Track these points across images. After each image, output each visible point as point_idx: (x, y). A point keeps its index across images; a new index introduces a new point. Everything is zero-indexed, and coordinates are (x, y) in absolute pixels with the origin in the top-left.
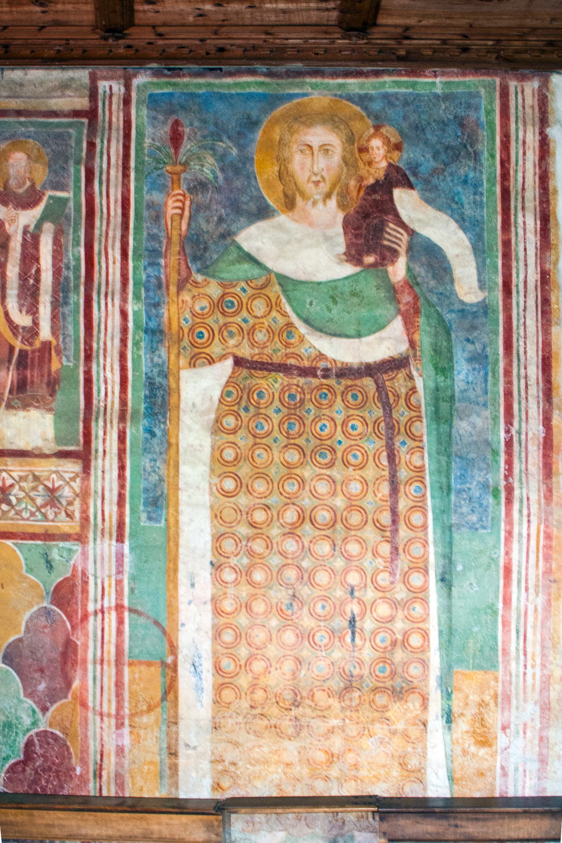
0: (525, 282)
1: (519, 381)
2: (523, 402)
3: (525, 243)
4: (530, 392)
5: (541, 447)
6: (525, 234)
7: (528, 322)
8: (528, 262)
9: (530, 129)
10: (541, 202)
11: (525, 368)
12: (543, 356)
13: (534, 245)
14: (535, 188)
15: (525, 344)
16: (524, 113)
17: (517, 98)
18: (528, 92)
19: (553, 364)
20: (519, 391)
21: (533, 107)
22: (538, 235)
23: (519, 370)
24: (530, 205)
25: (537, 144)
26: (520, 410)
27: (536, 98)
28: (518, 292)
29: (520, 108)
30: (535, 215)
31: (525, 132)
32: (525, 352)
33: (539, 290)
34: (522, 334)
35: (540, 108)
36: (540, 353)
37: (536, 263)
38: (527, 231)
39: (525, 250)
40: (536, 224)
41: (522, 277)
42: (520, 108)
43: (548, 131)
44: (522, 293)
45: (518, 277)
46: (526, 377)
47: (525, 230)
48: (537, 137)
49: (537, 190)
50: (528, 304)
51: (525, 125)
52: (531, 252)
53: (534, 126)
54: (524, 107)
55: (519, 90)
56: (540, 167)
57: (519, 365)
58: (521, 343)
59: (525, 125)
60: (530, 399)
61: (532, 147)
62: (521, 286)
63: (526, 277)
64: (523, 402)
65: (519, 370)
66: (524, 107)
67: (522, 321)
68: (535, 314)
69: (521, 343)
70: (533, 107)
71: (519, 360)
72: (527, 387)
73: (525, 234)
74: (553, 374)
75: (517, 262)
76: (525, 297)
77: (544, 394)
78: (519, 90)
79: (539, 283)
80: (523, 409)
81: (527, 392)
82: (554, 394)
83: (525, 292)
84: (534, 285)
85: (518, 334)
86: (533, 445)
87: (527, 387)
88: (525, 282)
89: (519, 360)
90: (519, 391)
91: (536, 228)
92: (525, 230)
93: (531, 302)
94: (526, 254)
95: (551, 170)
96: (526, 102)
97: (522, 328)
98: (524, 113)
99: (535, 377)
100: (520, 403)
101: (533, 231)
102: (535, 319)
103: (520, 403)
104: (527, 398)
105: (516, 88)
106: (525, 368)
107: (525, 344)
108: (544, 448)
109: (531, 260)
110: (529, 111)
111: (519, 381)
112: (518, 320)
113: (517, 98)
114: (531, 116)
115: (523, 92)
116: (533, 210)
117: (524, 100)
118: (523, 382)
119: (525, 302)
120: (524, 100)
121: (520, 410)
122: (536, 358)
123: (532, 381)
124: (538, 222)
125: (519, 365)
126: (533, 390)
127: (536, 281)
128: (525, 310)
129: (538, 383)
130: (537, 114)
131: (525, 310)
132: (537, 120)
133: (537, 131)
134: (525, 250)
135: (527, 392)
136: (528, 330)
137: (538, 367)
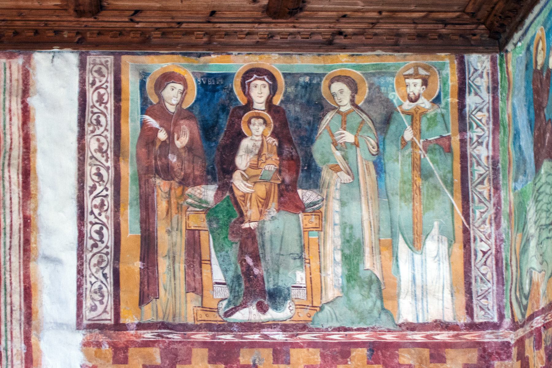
0: (11, 225)
1: (6, 307)
2: (9, 324)
3: (11, 193)
4: (14, 316)
5: (24, 361)
6: (10, 186)
7: (13, 259)
8: (13, 209)
9: (14, 99)
10: (24, 160)
11: (11, 296)
12: (25, 286)
13: (17, 195)
14: (19, 147)
15: (11, 277)
16: (11, 85)
17: (5, 73)
18: (14, 68)
19: (33, 293)
20: (6, 315)
21: (18, 80)
22: (21, 187)
23: (6, 298)
24: (14, 162)
25: (20, 112)
26: (6, 331)
27: (21, 73)
28: (5, 234)
29: (8, 81)
30: (18, 170)
31: (10, 101)
32: (11, 283)
33: (22, 232)
34: (8, 268)
35: (24, 81)
36: (22, 284)
37: (19, 209)
38: (12, 184)
39: (11, 199)
40: (18, 178)
41: (8, 221)
42: (8, 81)
43: (29, 100)
44: (8, 235)
45: (5, 221)
46: (11, 303)
47: (10, 183)
48: (20, 106)
49: (21, 148)
50: (13, 244)
51: (10, 95)
52: (15, 200)
53: (17, 96)
54: (11, 81)
55: (7, 66)
56: (23, 131)
57: (5, 294)
58: (8, 276)
59: (10, 95)
60: (14, 321)
61: (16, 114)
62: (8, 229)
63: (11, 221)
64: (9, 324)
65: (6, 298)
66: (11, 81)
67: (8, 258)
68: (18, 252)
69: (8, 276)
70: (18, 80)
71: (6, 290)
72: (12, 312)
73: (10, 186)
74: (33, 301)
75: (4, 209)
76: (11, 238)
77: (25, 318)
78: (7, 66)
79: (22, 226)
80: (8, 330)
81: (11, 316)
82: (33, 317)
83: (11, 234)
84: (18, 227)
85: (5, 268)
86: (17, 359)
87: (12, 312)
88: (11, 225)
89: (6, 290)
90: (6, 315)
91: (18, 181)
92: (10, 183)
93: (15, 242)
94: (11, 203)
95: (32, 132)
96: (13, 76)
97: (8, 263)
98: (11, 85)
99: (18, 303)
100: (6, 326)
101: (17, 184)
102: (18, 256)
103: (6, 326)
104: (11, 321)
105: (5, 64)
106: (11, 296)
107: (11, 277)
108: (26, 362)
109: (15, 207)
110: (14, 83)
111: (6, 307)
112: (5, 257)
113: (5, 73)
114: (16, 88)
115: (10, 68)
116: (16, 167)
117: (11, 74)
118: (9, 308)
119: (11, 242)
120: (11, 74)
121: (6, 331)
122: (19, 288)
123: (16, 307)
124: (20, 176)
125: (5, 294)
126: (16, 315)
127: (20, 224)
128: (10, 249)
129: (20, 309)
130: (21, 87)
131: (10, 249)
132: (20, 92)
133: (20, 100)
134: (11, 199)
135: (11, 316)
136: (13, 265)
137: (20, 296)
